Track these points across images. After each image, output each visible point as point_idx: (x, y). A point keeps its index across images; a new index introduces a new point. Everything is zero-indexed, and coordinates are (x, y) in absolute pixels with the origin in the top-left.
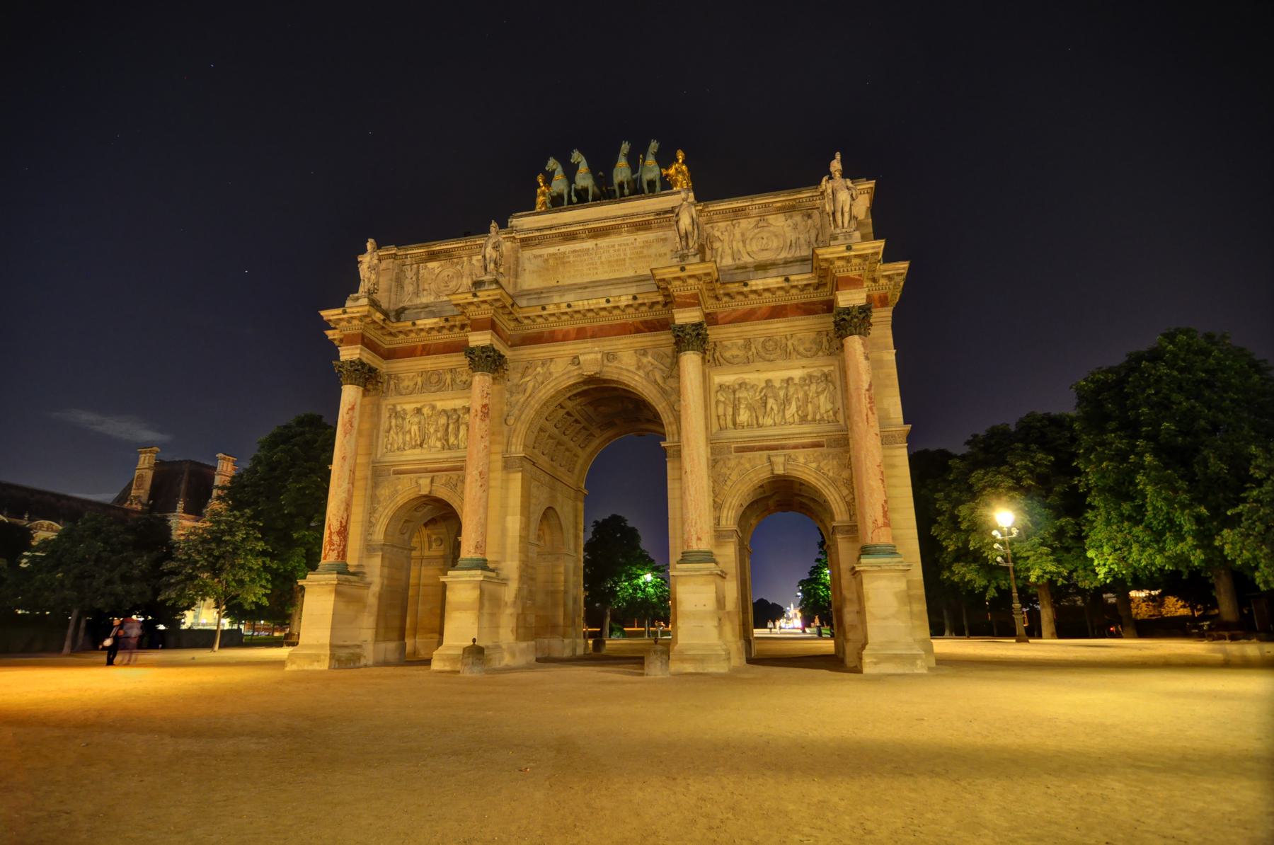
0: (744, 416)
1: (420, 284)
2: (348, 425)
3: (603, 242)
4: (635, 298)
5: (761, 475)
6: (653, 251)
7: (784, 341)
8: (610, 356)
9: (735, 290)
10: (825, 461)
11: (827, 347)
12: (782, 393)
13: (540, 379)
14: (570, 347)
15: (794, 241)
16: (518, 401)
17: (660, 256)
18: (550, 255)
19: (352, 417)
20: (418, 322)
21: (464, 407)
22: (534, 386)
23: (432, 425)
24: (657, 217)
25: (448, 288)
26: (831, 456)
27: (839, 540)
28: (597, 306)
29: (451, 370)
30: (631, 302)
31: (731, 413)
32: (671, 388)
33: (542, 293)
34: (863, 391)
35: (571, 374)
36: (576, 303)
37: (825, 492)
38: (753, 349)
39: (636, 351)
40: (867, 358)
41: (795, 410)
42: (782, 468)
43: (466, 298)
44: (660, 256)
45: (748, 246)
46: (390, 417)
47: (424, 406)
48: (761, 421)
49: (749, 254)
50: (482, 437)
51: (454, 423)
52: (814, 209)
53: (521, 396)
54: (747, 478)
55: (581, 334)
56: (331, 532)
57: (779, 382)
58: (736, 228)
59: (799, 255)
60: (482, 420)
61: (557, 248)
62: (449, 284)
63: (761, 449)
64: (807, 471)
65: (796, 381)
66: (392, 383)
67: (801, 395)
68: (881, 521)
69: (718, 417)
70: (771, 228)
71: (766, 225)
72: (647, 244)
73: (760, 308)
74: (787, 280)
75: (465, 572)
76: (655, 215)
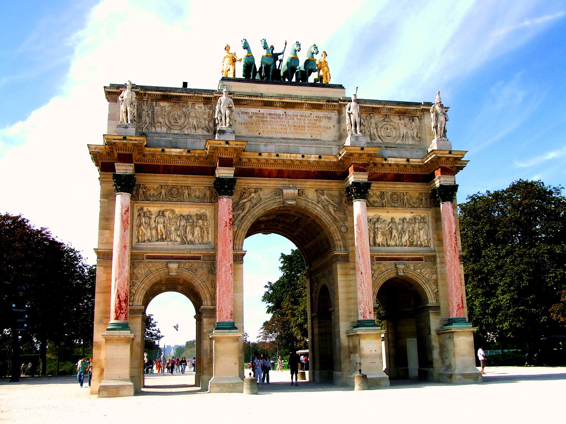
0: (379, 240)
1: (156, 117)
2: (126, 222)
3: (290, 112)
4: (320, 157)
5: (390, 275)
7: (402, 195)
8: (301, 193)
9: (379, 162)
10: (425, 269)
11: (425, 203)
12: (400, 227)
13: (254, 202)
14: (273, 182)
15: (405, 135)
16: (239, 214)
17: (327, 128)
19: (128, 217)
20: (166, 150)
21: (197, 215)
23: (173, 225)
24: (328, 103)
25: (176, 124)
26: (427, 266)
27: (430, 314)
28: (296, 159)
29: (188, 187)
30: (317, 160)
31: (372, 237)
32: (339, 217)
34: (453, 234)
35: (275, 201)
36: (282, 154)
37: (424, 286)
38: (386, 199)
39: (316, 191)
41: (408, 238)
42: (402, 272)
43: (221, 144)
44: (327, 128)
45: (379, 132)
46: (139, 215)
47: (166, 210)
48: (389, 243)
49: (380, 137)
50: (231, 241)
51: (190, 225)
52: (415, 116)
53: (240, 212)
54: (383, 276)
55: (280, 174)
56: (120, 302)
57: (399, 220)
58: (372, 119)
59: (407, 143)
61: (259, 109)
62: (178, 121)
63: (390, 259)
64: (415, 274)
65: (408, 220)
66: (141, 191)
67: (411, 229)
68: (461, 306)
70: (392, 123)
71: (389, 121)
73: (389, 174)
74: (408, 160)
75: (227, 331)
76: (326, 102)
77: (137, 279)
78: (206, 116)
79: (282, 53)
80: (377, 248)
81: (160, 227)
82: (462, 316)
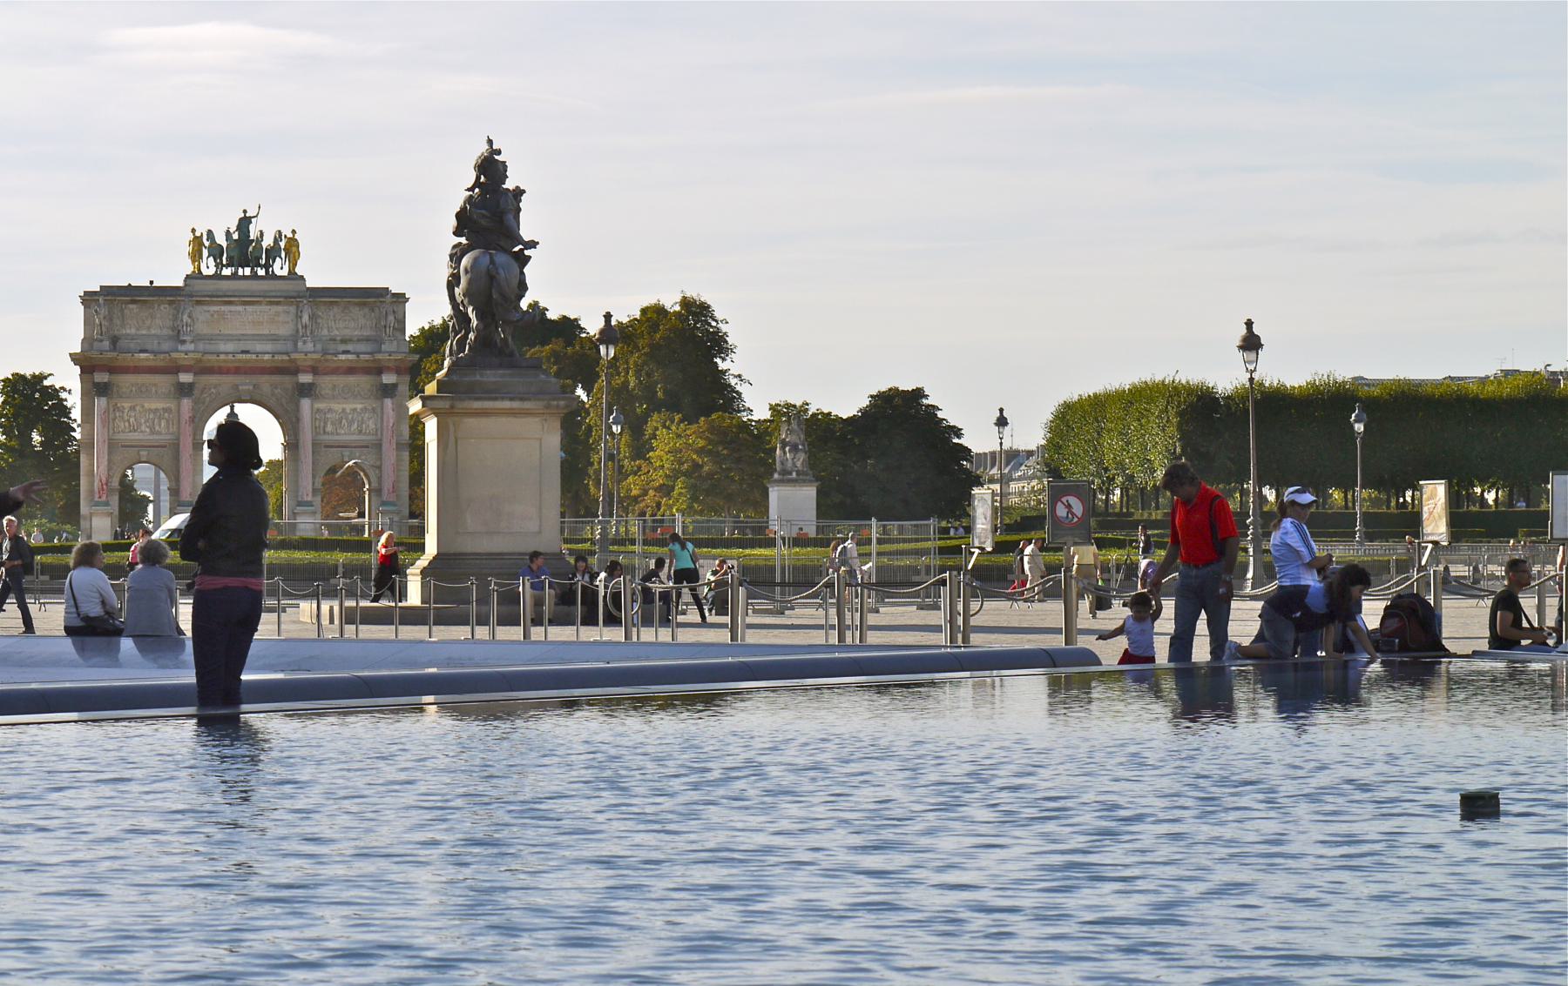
0: (329, 428)
3: (250, 308)
6: (281, 319)
12: (350, 416)
14: (231, 378)
18: (214, 311)
21: (163, 409)
22: (210, 401)
29: (155, 385)
33: (212, 340)
39: (271, 385)
40: (393, 410)
46: (114, 410)
55: (237, 371)
60: (189, 425)
67: (360, 419)
68: (391, 490)
69: (316, 428)
72: (277, 314)
77: (114, 464)
78: (171, 317)
79: (256, 216)
80: (326, 437)
81: (132, 420)
82: (391, 500)
